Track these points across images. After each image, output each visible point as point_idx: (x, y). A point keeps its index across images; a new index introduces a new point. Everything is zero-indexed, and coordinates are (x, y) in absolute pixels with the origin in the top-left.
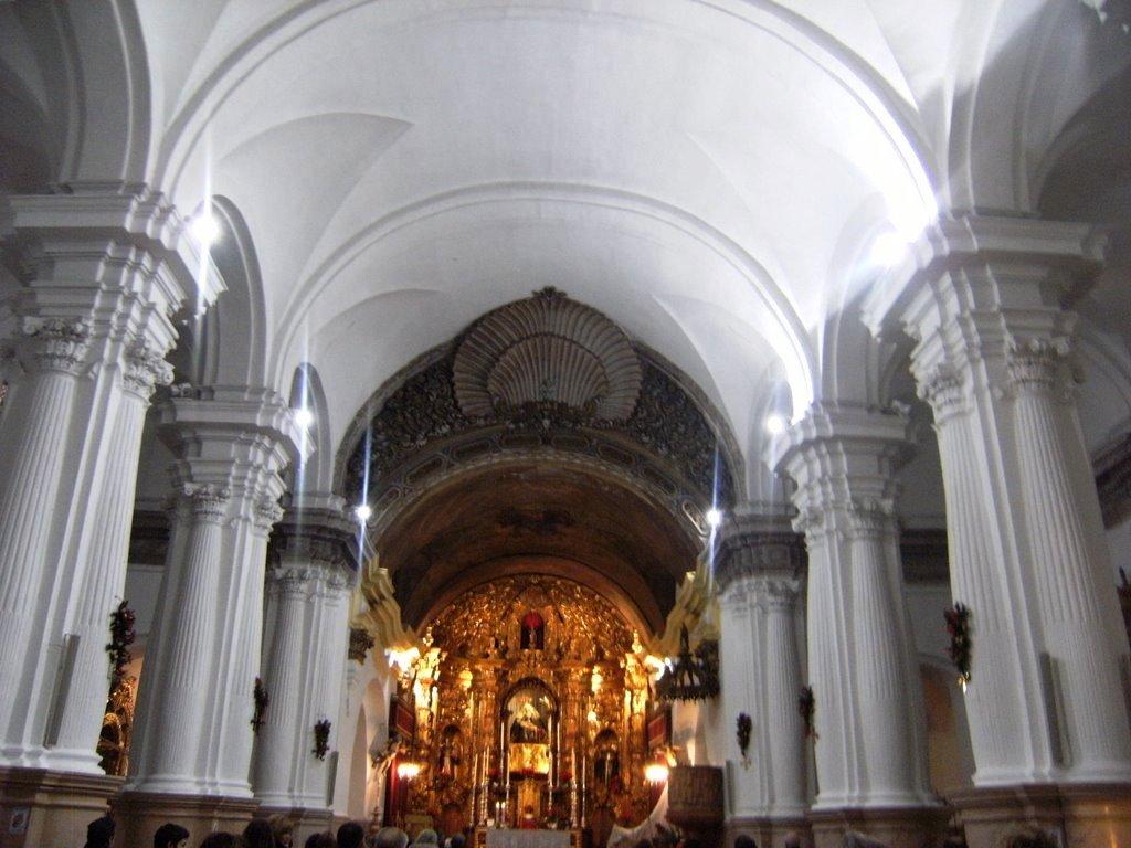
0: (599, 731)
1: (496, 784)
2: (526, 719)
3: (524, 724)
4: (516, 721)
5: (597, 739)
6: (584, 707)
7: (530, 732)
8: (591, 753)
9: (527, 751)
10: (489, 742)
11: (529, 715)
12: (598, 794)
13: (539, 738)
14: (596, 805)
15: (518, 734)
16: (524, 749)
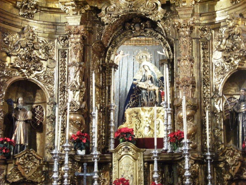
0: (227, 75)
1: (81, 153)
2: (144, 80)
3: (142, 85)
4: (133, 85)
5: (225, 88)
6: (206, 45)
7: (150, 94)
8: (219, 107)
9: (145, 113)
10: (73, 97)
11: (149, 74)
12: (229, 161)
13: (155, 101)
14: (227, 177)
15: (135, 96)
16: (142, 113)
